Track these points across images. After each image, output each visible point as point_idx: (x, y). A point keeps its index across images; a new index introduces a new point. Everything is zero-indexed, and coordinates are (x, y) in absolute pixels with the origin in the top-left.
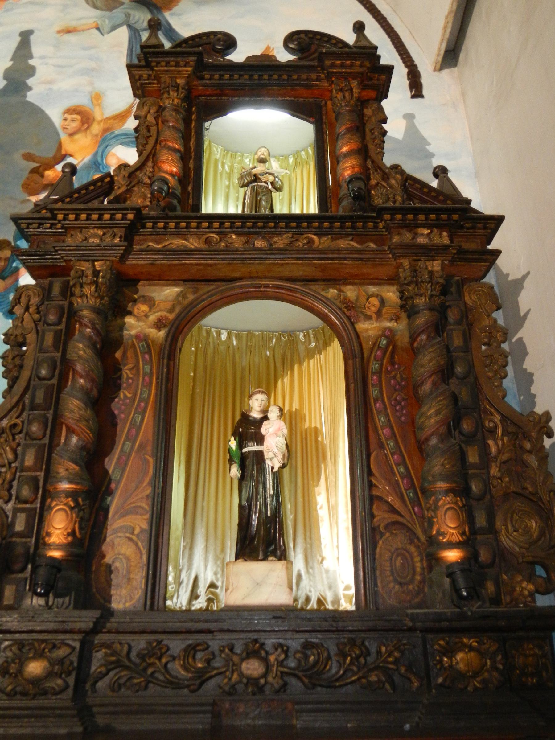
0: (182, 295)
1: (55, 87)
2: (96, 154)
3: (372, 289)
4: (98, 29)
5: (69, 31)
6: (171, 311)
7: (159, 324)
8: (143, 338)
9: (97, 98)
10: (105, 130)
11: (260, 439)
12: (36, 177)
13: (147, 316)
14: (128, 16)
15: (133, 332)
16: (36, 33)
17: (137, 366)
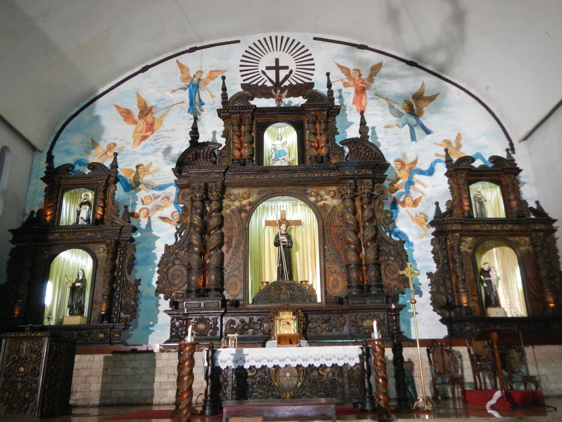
0: (473, 240)
1: (389, 151)
2: (409, 178)
3: (522, 238)
4: (398, 126)
5: (388, 127)
6: (471, 244)
7: (469, 248)
8: (466, 252)
9: (404, 155)
10: (410, 168)
11: (489, 276)
12: (391, 186)
13: (465, 246)
14: (407, 119)
15: (463, 250)
16: (376, 127)
17: (466, 260)
